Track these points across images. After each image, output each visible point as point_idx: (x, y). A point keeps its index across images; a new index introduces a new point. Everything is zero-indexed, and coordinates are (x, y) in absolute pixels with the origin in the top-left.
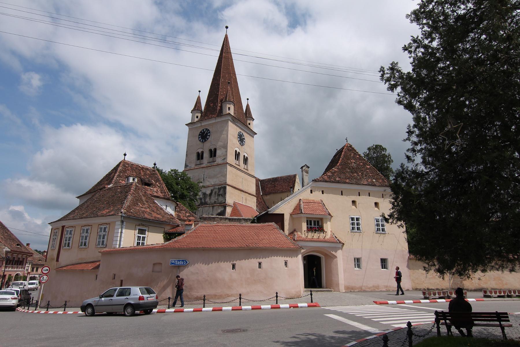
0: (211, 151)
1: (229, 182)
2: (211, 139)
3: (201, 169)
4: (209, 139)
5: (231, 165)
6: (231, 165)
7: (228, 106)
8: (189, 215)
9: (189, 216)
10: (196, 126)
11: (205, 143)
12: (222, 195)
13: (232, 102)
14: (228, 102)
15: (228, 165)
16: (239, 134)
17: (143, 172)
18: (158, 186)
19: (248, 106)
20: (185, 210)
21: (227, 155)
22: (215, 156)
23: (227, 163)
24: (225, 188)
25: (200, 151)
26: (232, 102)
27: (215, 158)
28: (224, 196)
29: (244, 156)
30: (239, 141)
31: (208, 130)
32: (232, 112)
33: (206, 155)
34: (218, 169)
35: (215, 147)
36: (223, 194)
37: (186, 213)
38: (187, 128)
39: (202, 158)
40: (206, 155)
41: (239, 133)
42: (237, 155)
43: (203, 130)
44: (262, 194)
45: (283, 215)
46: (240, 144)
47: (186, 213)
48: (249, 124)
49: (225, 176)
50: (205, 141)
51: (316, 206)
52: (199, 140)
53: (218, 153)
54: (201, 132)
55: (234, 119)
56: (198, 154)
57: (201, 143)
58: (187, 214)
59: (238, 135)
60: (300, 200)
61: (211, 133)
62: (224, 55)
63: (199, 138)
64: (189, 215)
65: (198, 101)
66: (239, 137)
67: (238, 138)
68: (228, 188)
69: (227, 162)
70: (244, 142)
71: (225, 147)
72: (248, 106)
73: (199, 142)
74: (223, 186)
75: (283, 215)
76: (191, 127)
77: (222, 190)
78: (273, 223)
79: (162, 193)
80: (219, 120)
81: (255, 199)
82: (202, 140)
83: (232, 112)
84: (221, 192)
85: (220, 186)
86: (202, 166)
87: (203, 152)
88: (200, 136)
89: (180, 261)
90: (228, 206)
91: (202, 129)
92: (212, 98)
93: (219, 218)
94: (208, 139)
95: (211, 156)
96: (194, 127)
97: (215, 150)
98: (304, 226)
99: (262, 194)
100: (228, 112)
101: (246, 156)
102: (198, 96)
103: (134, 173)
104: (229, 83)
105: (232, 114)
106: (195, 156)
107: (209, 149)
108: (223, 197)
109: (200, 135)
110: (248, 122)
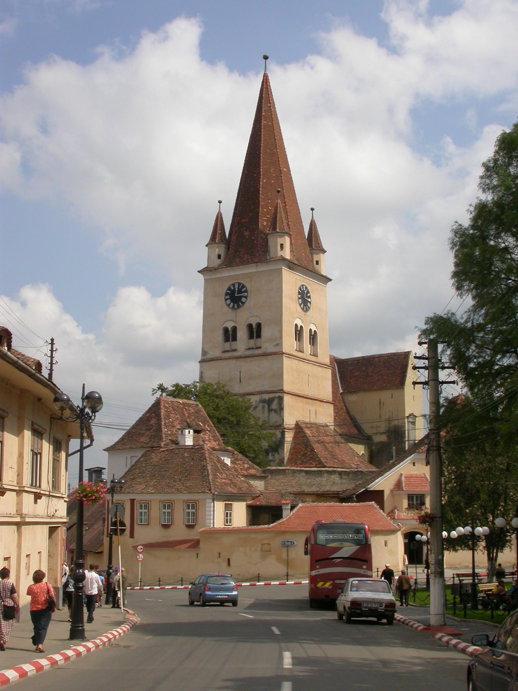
0: (250, 326)
1: (286, 388)
2: (250, 303)
3: (234, 361)
4: (247, 304)
5: (290, 355)
6: (290, 355)
7: (280, 241)
8: (248, 466)
9: (249, 468)
10: (218, 275)
11: (239, 311)
12: (275, 411)
13: (287, 233)
14: (279, 234)
15: (284, 357)
16: (301, 290)
17: (186, 411)
18: (209, 431)
19: (313, 225)
20: (241, 460)
21: (281, 338)
22: (259, 336)
23: (284, 353)
24: (281, 399)
25: (230, 325)
26: (287, 233)
27: (258, 339)
28: (280, 414)
29: (311, 330)
30: (300, 305)
31: (244, 286)
32: (287, 254)
33: (242, 334)
34: (265, 363)
35: (258, 321)
36: (278, 410)
37: (243, 463)
38: (201, 278)
39: (235, 339)
40: (242, 334)
41: (300, 289)
42: (299, 332)
43: (234, 285)
44: (341, 391)
45: (382, 492)
46: (303, 309)
47: (243, 463)
48: (317, 263)
49: (280, 376)
50: (239, 307)
51: (418, 481)
52: (227, 304)
53: (266, 332)
54: (229, 289)
55: (291, 265)
56: (226, 330)
57: (230, 310)
58: (246, 466)
59: (299, 293)
60: (401, 475)
61: (249, 291)
62: (263, 122)
63: (226, 300)
64: (248, 466)
65: (219, 219)
66: (300, 296)
67: (299, 298)
68: (287, 399)
69: (284, 351)
70: (309, 304)
71: (278, 322)
72: (313, 225)
73: (226, 309)
74: (277, 395)
75: (382, 492)
76: (208, 277)
77: (276, 401)
78: (373, 502)
79: (215, 441)
80: (263, 268)
81: (330, 409)
82: (232, 305)
83: (287, 254)
84: (274, 406)
85: (271, 396)
86: (235, 354)
87: (235, 329)
88: (228, 297)
89: (288, 542)
90: (287, 431)
91: (232, 283)
92: (246, 219)
93: (291, 470)
94: (243, 303)
95: (251, 336)
96: (212, 277)
97: (259, 325)
98: (405, 503)
99: (341, 391)
100: (280, 253)
101: (314, 328)
102: (218, 212)
103: (178, 416)
104: (279, 192)
105: (288, 256)
106: (219, 336)
107: (247, 323)
108: (277, 414)
109: (227, 294)
110: (316, 258)
